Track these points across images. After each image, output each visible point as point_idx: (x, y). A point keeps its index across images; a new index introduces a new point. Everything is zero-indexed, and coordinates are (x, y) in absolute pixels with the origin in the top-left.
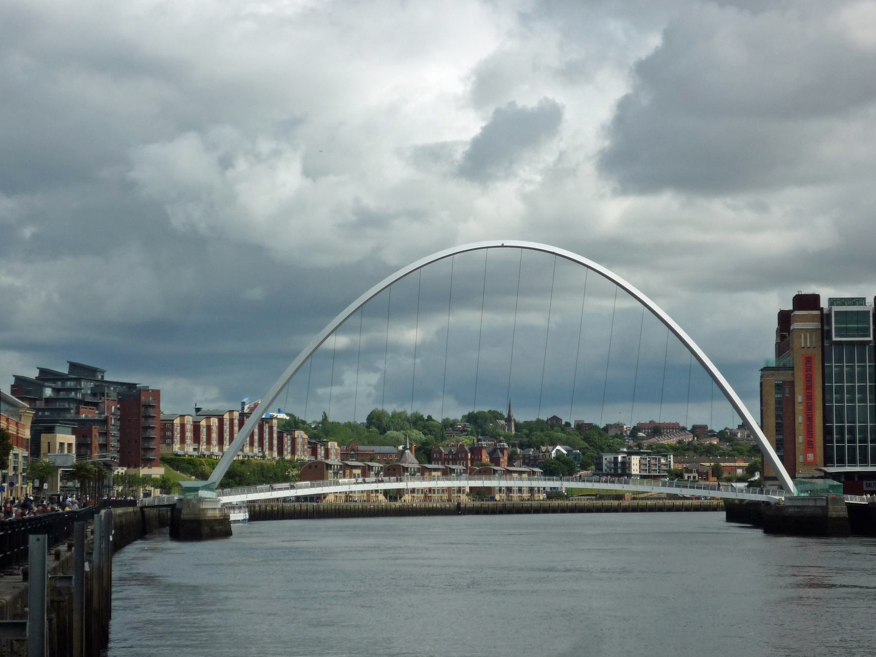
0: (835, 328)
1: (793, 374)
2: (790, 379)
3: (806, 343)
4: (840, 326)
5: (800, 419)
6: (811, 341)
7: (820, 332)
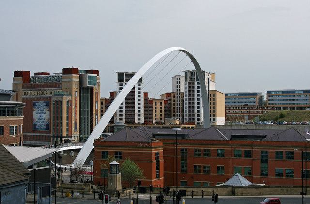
2: (71, 99)
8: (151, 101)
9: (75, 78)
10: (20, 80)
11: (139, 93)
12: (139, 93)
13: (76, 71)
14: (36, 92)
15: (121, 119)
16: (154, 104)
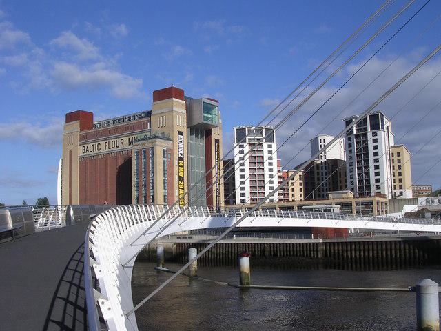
10: (76, 125)
13: (179, 94)
14: (103, 143)
15: (243, 201)
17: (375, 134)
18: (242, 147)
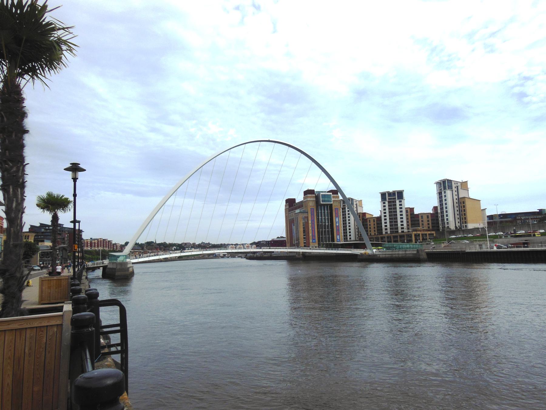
0: (322, 200)
1: (308, 214)
2: (307, 216)
3: (311, 205)
4: (336, 195)
5: (310, 228)
6: (313, 204)
7: (315, 201)
8: (417, 215)
9: (311, 198)
11: (401, 208)
12: (401, 208)
16: (420, 217)
17: (445, 192)
18: (384, 203)
